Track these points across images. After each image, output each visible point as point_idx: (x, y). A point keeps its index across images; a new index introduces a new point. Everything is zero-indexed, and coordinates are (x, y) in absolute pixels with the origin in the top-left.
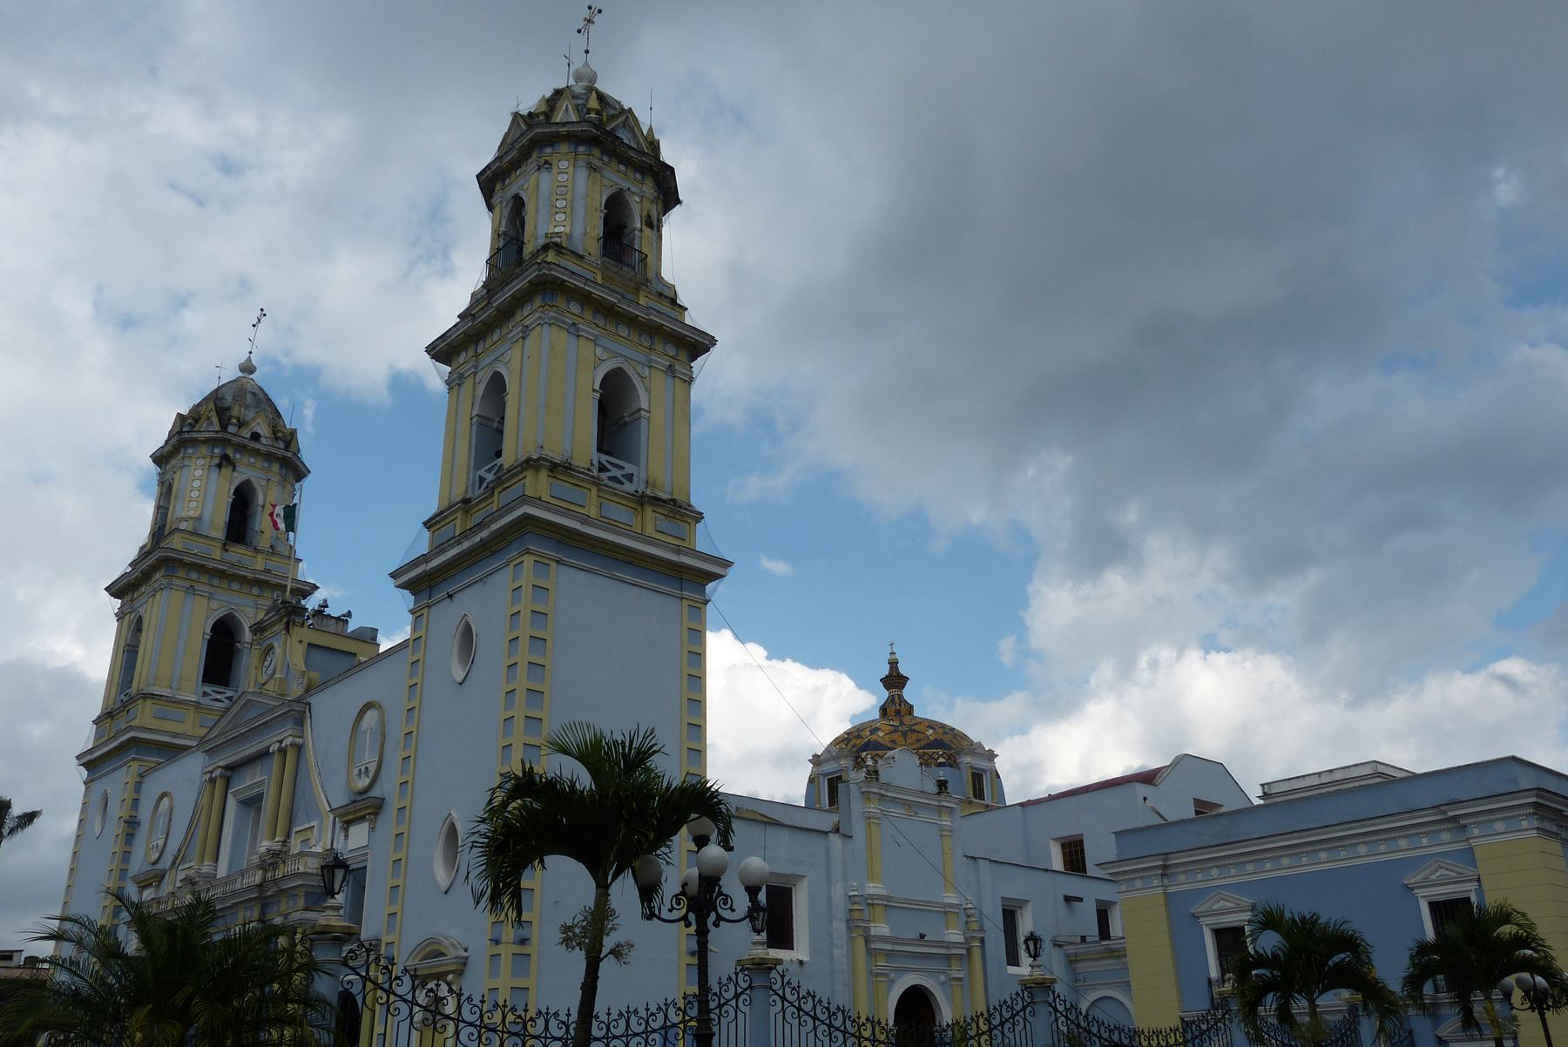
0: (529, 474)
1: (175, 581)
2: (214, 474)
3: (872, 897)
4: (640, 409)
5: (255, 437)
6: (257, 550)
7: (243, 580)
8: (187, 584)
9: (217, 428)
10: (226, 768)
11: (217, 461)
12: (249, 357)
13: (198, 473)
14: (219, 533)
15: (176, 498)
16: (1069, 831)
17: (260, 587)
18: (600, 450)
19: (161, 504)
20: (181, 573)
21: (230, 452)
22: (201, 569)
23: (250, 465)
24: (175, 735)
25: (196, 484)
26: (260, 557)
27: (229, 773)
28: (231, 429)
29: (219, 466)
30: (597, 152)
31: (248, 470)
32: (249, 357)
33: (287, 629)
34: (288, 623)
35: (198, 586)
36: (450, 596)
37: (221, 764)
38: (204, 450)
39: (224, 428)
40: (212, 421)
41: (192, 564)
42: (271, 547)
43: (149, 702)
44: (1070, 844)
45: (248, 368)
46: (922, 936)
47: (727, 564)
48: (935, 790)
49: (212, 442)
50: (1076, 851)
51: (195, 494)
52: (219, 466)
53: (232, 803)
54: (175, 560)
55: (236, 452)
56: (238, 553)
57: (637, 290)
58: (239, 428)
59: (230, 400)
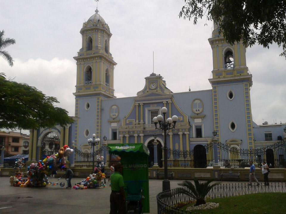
8: (103, 62)
10: (143, 103)
13: (99, 36)
35: (105, 62)
45: (97, 11)
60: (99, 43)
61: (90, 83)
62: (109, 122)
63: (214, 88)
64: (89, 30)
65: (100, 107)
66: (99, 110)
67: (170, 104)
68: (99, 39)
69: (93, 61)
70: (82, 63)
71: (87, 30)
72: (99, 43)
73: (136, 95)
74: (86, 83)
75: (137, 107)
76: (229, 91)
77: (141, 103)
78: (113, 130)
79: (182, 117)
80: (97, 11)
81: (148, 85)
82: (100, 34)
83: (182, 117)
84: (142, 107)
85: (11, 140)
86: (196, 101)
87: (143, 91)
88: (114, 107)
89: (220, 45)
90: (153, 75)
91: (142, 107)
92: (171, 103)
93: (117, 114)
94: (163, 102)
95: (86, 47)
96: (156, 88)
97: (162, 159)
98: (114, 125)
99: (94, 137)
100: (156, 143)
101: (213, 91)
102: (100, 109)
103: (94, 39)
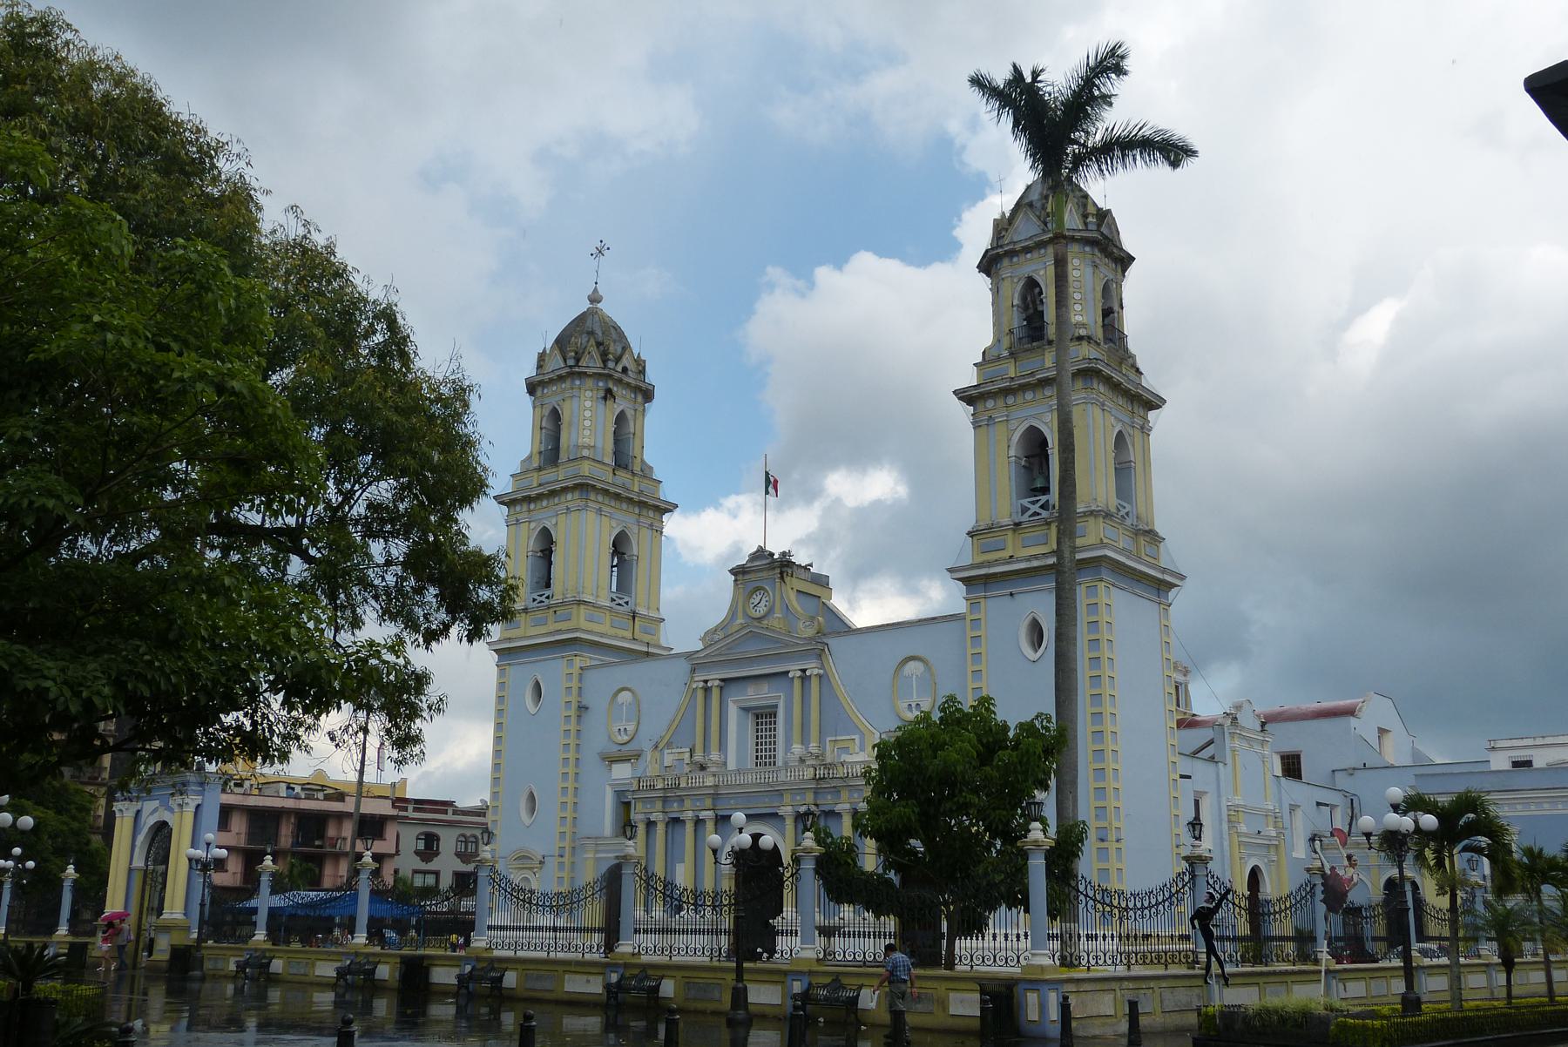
0: (1091, 520)
1: (590, 504)
2: (601, 406)
3: (1238, 806)
4: (1131, 461)
5: (625, 370)
6: (634, 474)
7: (630, 500)
9: (599, 364)
10: (722, 680)
11: (602, 394)
12: (596, 288)
13: (588, 404)
14: (609, 460)
15: (570, 424)
16: (1289, 748)
17: (639, 507)
18: (1118, 497)
19: (544, 425)
20: (592, 496)
21: (611, 385)
22: (606, 492)
23: (624, 397)
24: (602, 635)
25: (588, 414)
26: (636, 479)
27: (722, 684)
28: (611, 365)
29: (605, 398)
30: (1096, 251)
31: (624, 401)
32: (596, 288)
33: (782, 578)
34: (781, 573)
35: (604, 508)
36: (1011, 594)
37: (717, 676)
38: (590, 382)
39: (605, 367)
40: (592, 356)
41: (602, 489)
42: (642, 471)
43: (582, 607)
44: (1288, 757)
45: (595, 298)
46: (1259, 832)
47: (1182, 577)
48: (1260, 729)
49: (598, 376)
50: (1294, 763)
51: (587, 423)
52: (605, 398)
53: (733, 712)
54: (588, 485)
55: (614, 384)
56: (623, 476)
57: (1121, 363)
58: (616, 364)
59: (600, 334)
60: (587, 433)
61: (548, 598)
62: (604, 759)
63: (973, 604)
64: (551, 381)
65: (573, 699)
66: (573, 712)
67: (815, 683)
68: (588, 414)
69: (557, 508)
70: (523, 517)
71: (542, 384)
72: (587, 433)
73: (700, 646)
74: (534, 600)
75: (700, 694)
76: (1030, 617)
77: (715, 676)
78: (619, 794)
79: (856, 737)
80: (595, 298)
81: (740, 604)
82: (589, 394)
83: (856, 737)
84: (715, 693)
85: (348, 829)
86: (912, 665)
87: (723, 626)
88: (625, 697)
89: (999, 416)
90: (761, 553)
91: (715, 693)
92: (820, 676)
93: (631, 728)
94: (790, 675)
95: (540, 453)
96: (770, 611)
97: (771, 921)
98: (622, 772)
99: (208, 844)
100: (368, 864)
101: (968, 619)
102: (574, 706)
103: (565, 417)
